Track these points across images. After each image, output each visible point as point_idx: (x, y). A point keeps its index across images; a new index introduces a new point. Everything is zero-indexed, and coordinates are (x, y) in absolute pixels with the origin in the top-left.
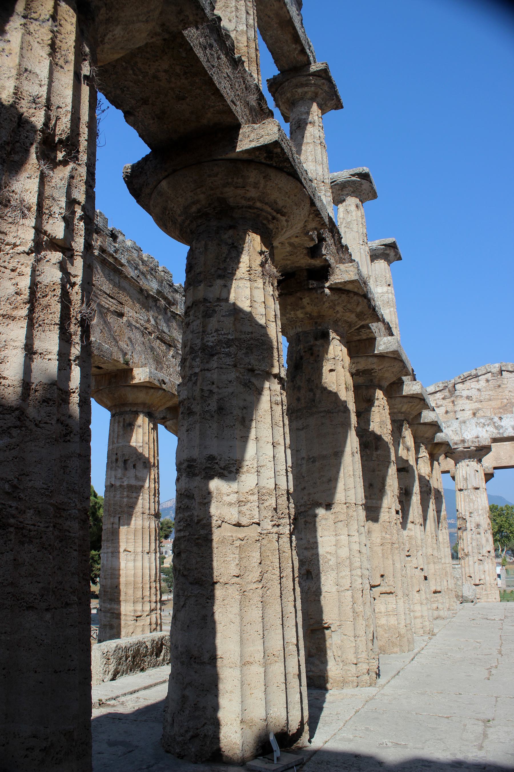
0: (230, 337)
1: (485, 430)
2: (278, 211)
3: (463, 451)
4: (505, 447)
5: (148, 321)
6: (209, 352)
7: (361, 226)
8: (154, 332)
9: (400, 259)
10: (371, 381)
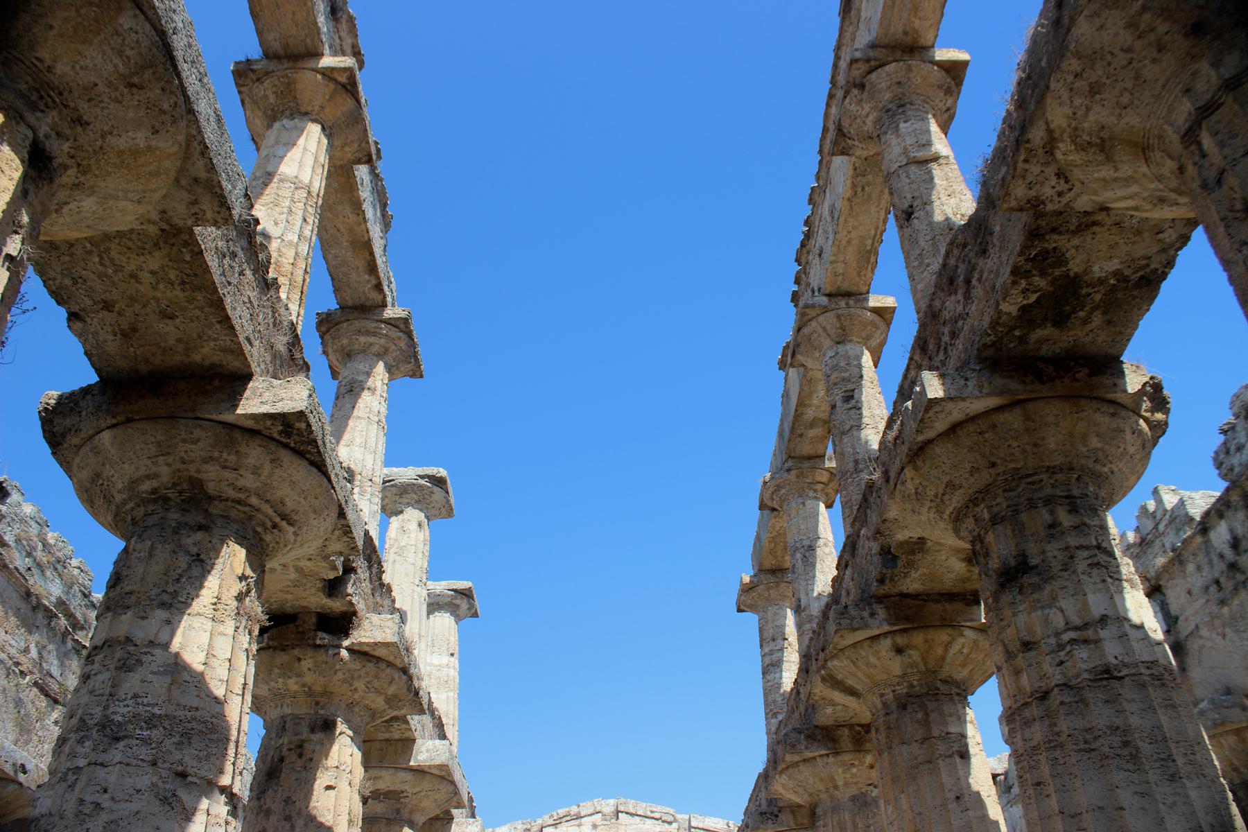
0: (157, 711)
2: (284, 517)
5: (26, 650)
6: (112, 732)
7: (420, 555)
8: (31, 673)
9: (475, 615)
10: (398, 811)
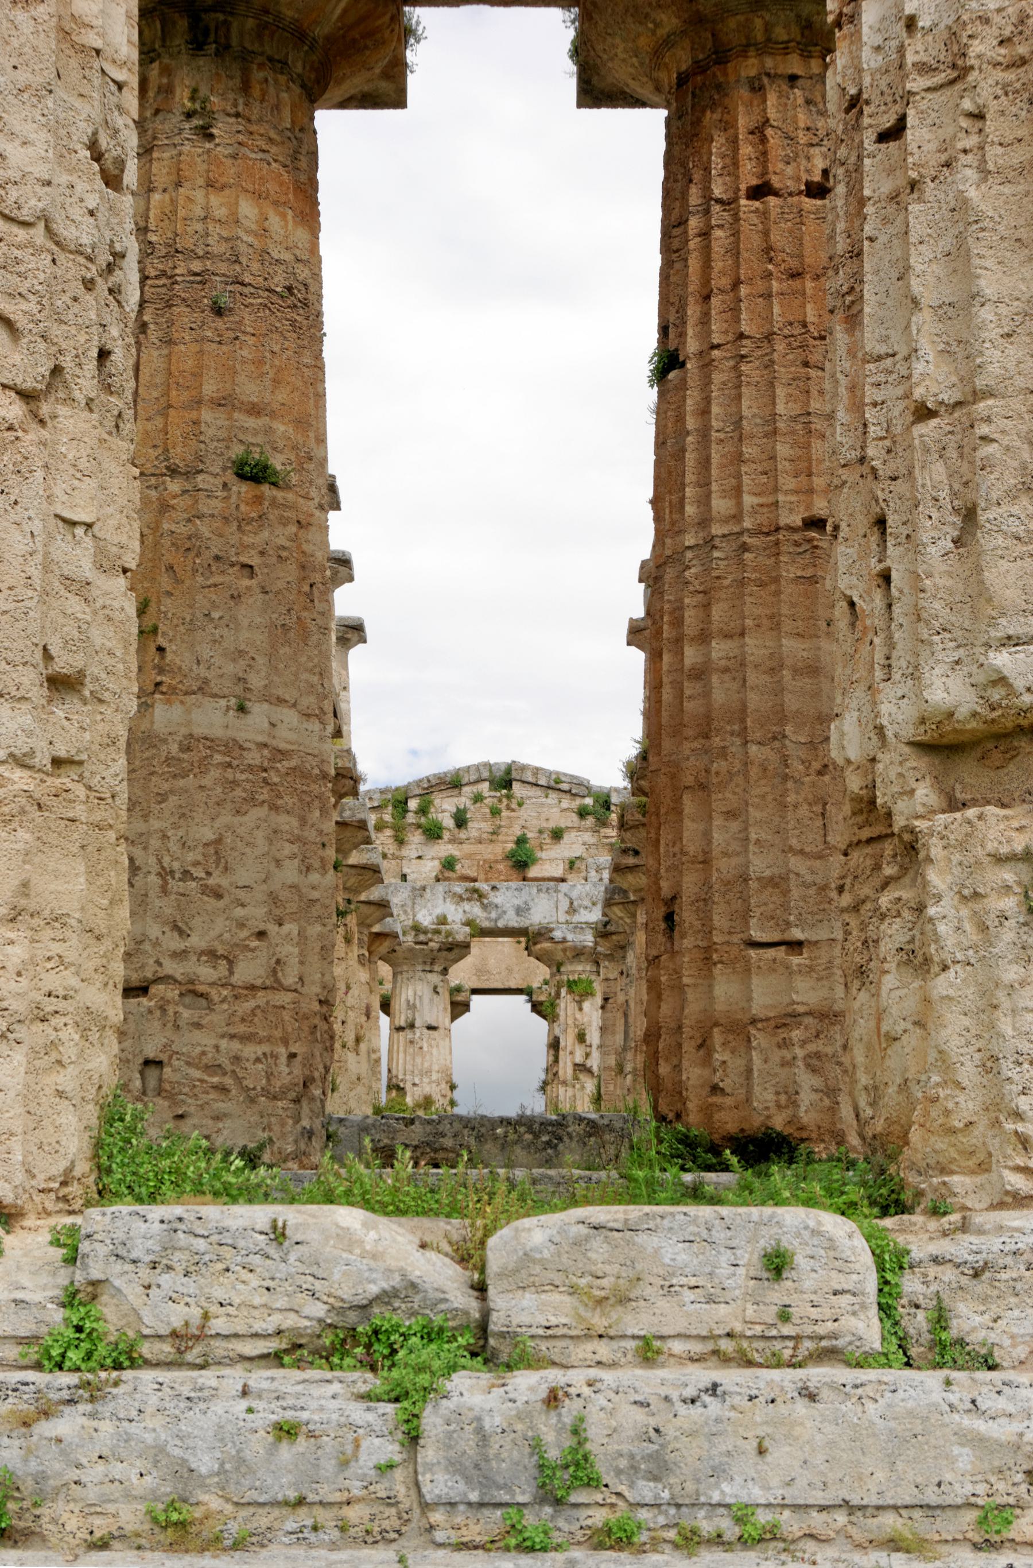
1: (461, 911)
3: (411, 950)
4: (500, 947)
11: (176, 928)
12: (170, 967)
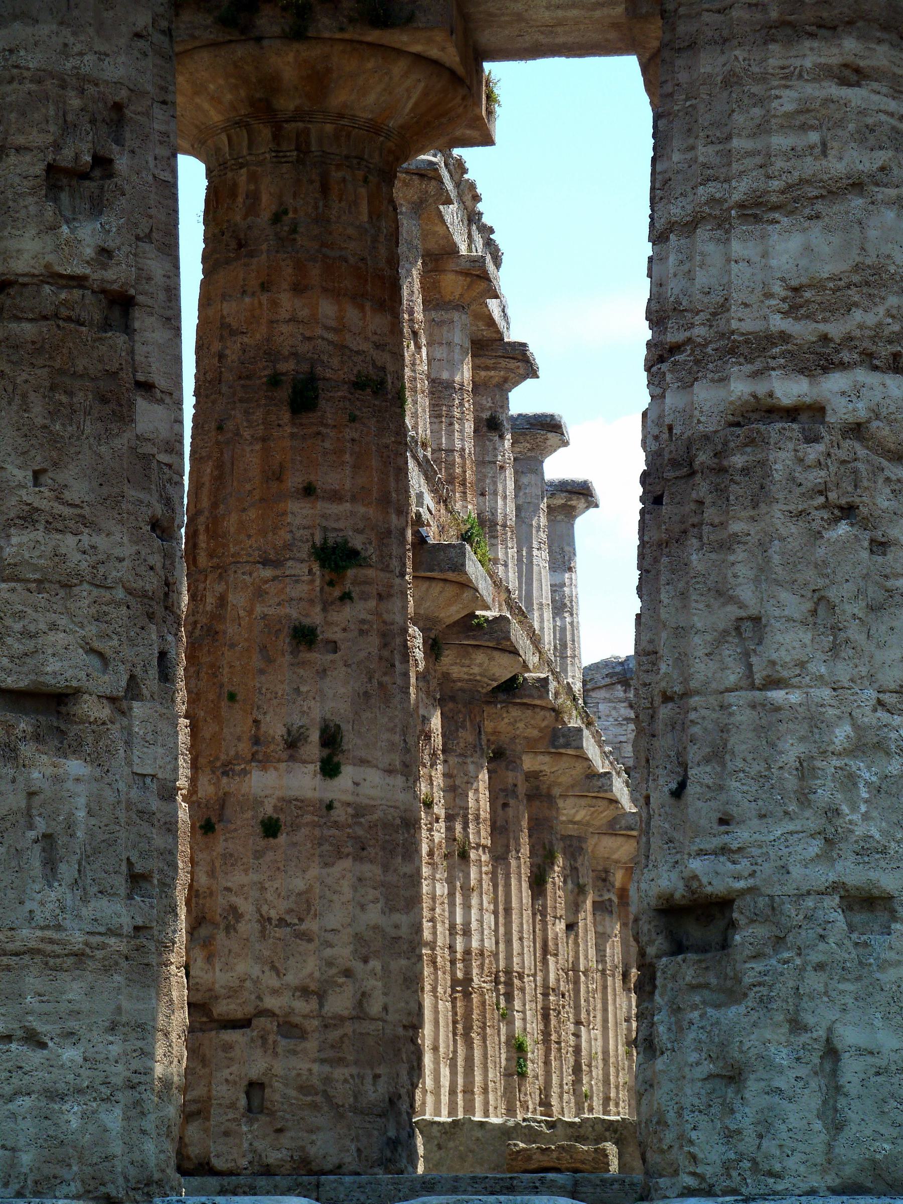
11: (273, 968)
12: (270, 1002)
